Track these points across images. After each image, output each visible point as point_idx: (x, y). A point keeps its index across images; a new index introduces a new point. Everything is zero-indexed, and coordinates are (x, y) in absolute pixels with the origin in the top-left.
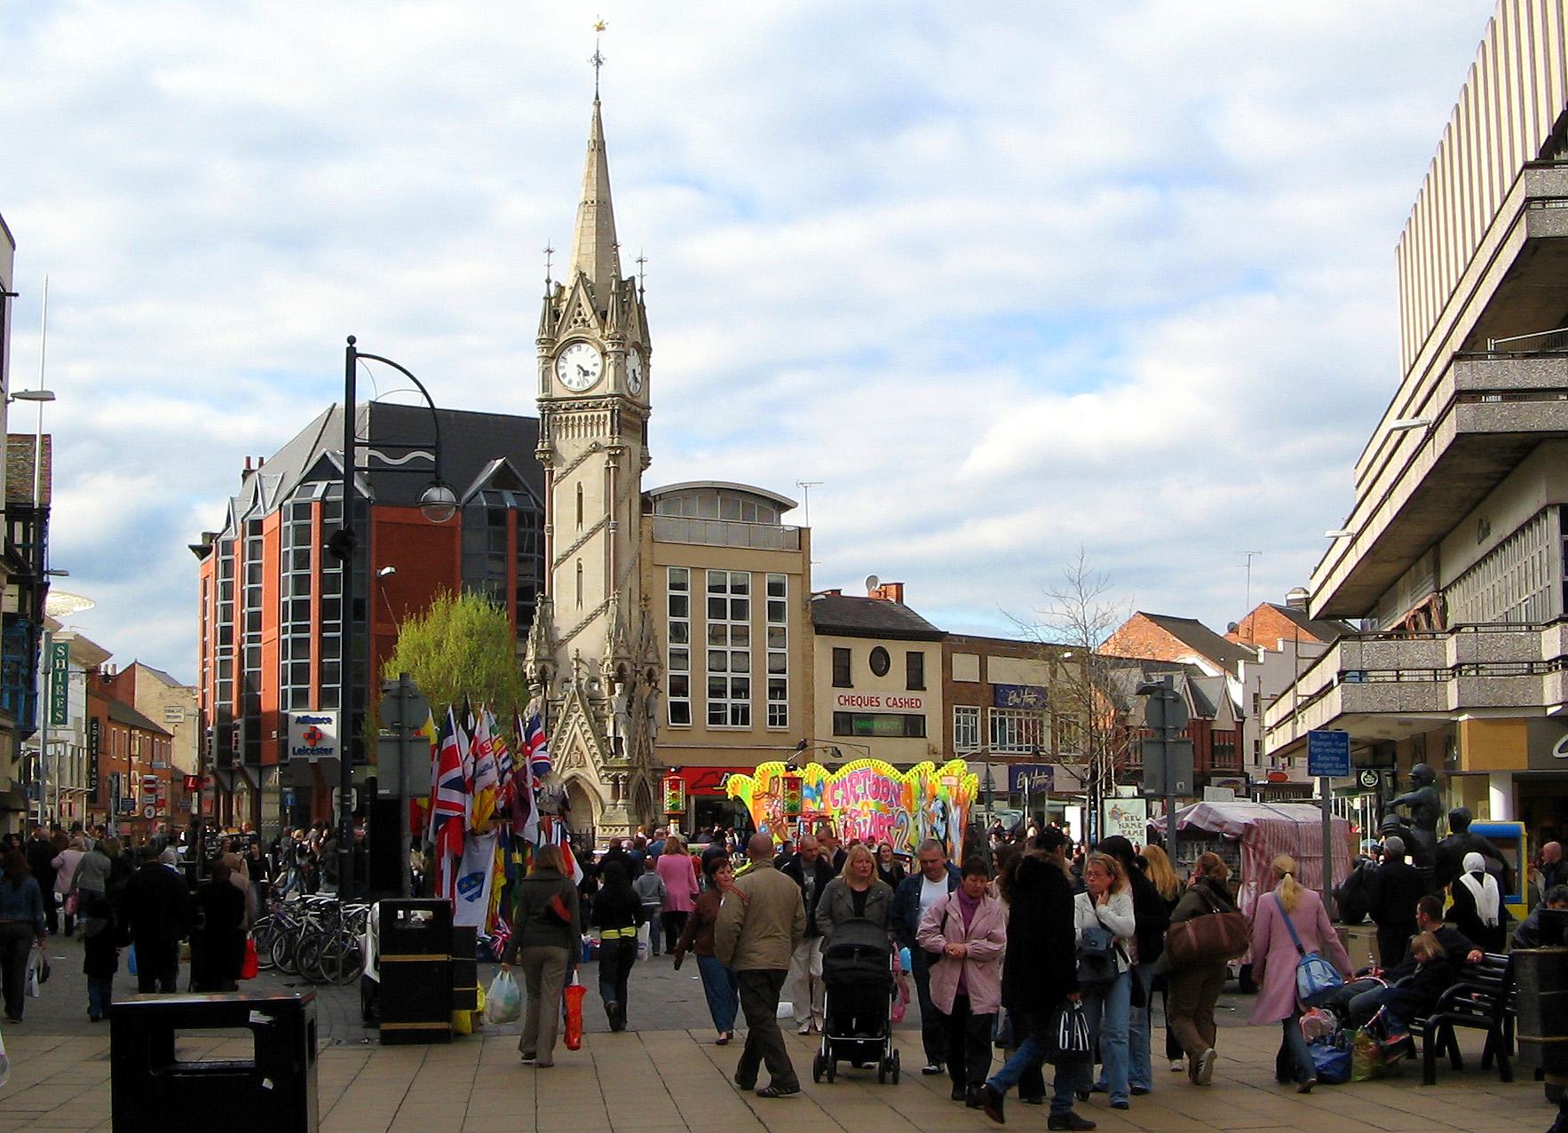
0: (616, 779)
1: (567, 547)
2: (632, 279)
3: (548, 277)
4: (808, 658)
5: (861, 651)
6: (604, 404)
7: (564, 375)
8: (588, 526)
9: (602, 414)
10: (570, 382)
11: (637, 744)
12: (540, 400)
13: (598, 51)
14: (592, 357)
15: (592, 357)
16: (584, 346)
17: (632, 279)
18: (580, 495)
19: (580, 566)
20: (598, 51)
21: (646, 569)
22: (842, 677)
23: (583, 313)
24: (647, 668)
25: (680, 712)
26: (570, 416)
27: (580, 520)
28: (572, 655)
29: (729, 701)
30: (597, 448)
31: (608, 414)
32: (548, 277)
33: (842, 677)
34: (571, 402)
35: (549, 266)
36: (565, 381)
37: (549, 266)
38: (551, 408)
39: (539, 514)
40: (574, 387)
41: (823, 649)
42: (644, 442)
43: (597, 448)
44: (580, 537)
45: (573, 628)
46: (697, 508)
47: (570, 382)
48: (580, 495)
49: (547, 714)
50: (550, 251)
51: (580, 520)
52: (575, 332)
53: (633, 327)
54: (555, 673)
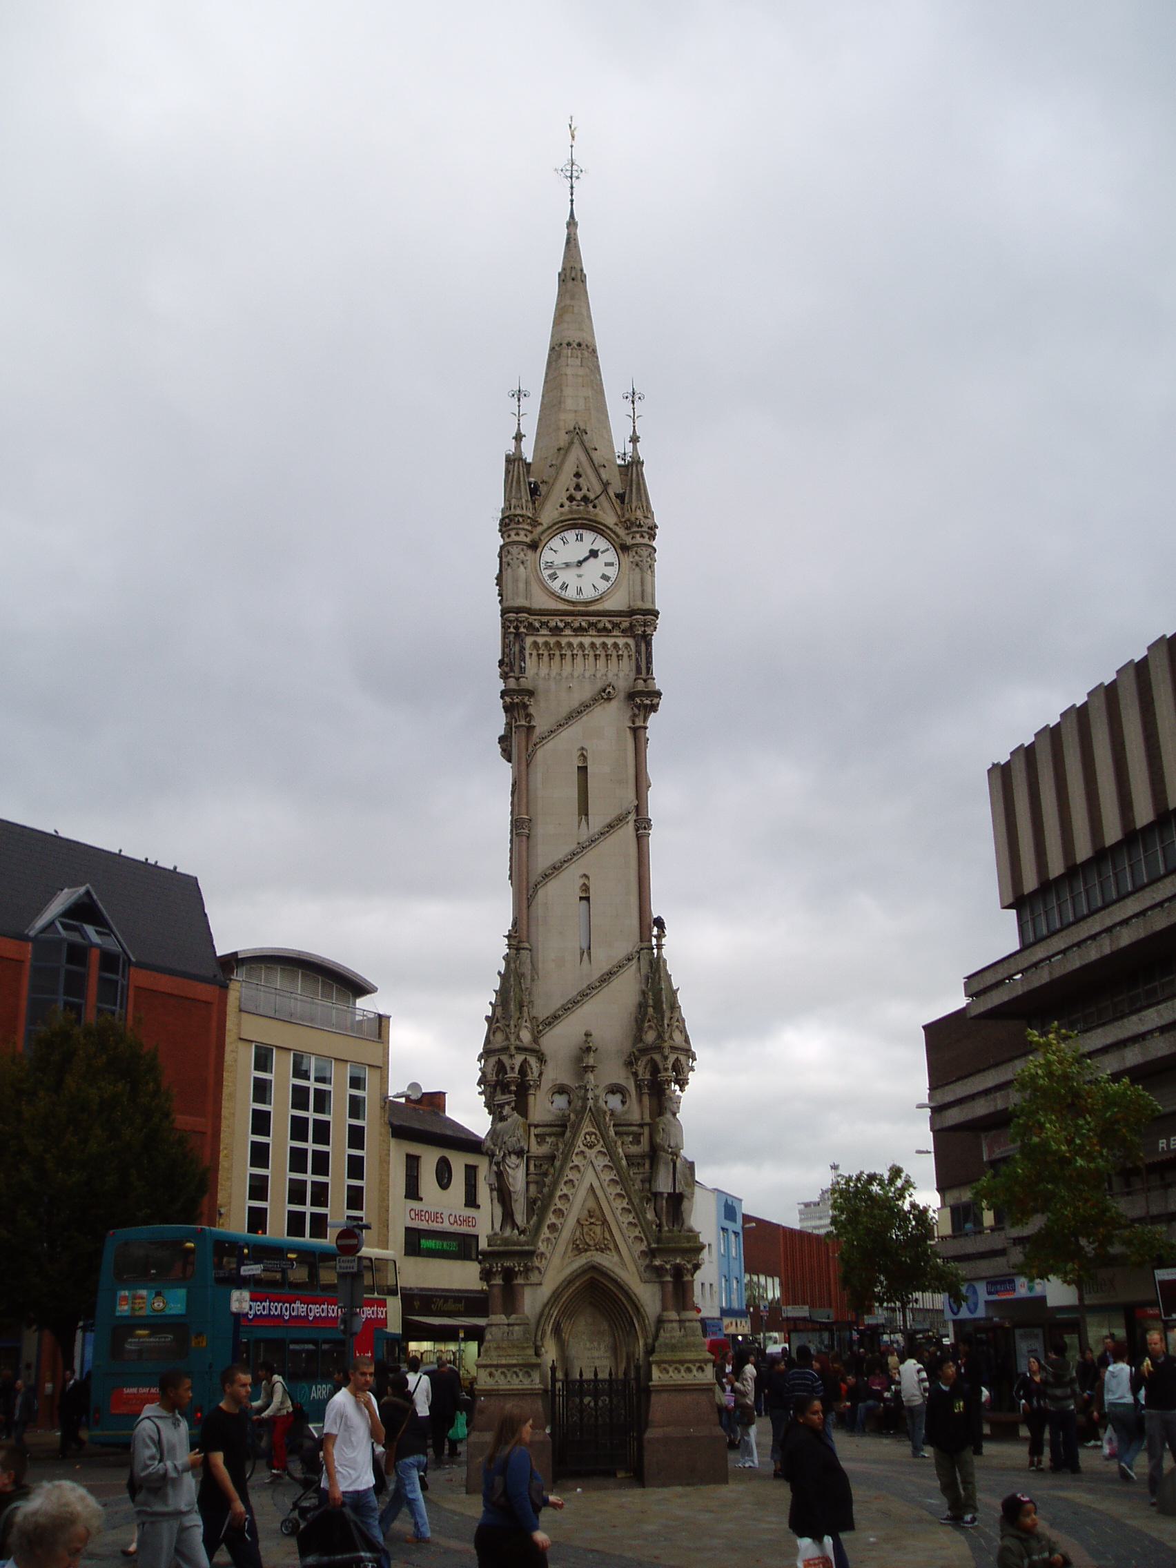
3: (519, 429)
4: (384, 1162)
5: (430, 1158)
6: (625, 625)
8: (598, 820)
18: (583, 770)
21: (231, 1043)
22: (413, 1192)
25: (257, 1219)
27: (584, 810)
29: (308, 1209)
30: (604, 695)
32: (519, 429)
33: (413, 1192)
34: (569, 619)
38: (531, 624)
41: (398, 1152)
43: (604, 695)
44: (584, 837)
46: (278, 979)
48: (583, 770)
51: (584, 810)
54: (541, 1074)
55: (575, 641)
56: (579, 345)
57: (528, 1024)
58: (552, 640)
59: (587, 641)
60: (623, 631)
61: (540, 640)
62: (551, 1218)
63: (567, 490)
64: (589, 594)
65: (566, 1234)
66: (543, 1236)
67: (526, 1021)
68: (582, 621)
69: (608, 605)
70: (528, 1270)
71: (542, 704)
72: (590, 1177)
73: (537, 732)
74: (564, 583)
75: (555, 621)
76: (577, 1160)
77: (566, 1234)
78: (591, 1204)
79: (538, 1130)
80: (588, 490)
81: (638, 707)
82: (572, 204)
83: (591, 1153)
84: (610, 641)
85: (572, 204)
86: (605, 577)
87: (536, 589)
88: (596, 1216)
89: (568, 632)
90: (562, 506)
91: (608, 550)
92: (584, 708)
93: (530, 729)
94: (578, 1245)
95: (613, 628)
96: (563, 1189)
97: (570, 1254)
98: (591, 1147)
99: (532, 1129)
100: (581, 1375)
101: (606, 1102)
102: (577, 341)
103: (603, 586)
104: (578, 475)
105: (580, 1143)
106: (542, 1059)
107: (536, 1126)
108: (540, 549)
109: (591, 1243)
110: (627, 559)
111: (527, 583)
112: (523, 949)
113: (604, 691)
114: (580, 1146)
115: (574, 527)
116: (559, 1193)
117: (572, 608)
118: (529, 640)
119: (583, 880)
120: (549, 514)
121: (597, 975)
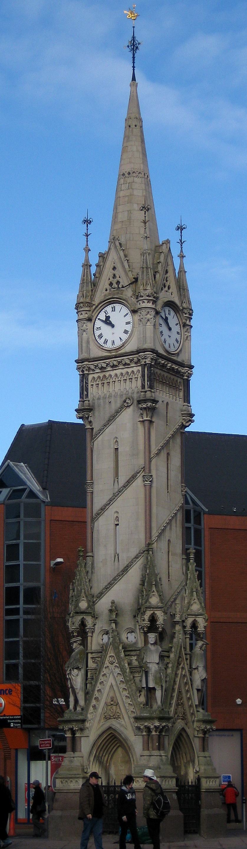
0: (148, 729)
1: (104, 502)
2: (168, 242)
7: (100, 336)
8: (122, 480)
9: (135, 369)
10: (106, 342)
11: (175, 694)
12: (77, 361)
13: (134, 37)
14: (125, 316)
15: (125, 316)
16: (118, 306)
17: (168, 242)
19: (117, 518)
20: (134, 37)
23: (117, 276)
24: (190, 621)
26: (107, 374)
28: (108, 606)
31: (140, 368)
35: (87, 235)
36: (101, 342)
37: (87, 235)
38: (89, 368)
39: (195, 511)
40: (109, 346)
42: (187, 399)
45: (110, 579)
47: (106, 342)
49: (87, 666)
50: (87, 222)
52: (110, 294)
53: (169, 288)
55: (113, 373)
56: (129, 173)
57: (85, 599)
58: (101, 375)
59: (118, 372)
60: (136, 363)
61: (96, 376)
62: (94, 702)
63: (109, 279)
64: (118, 343)
65: (100, 710)
66: (90, 712)
67: (83, 597)
68: (114, 362)
69: (128, 349)
70: (82, 730)
71: (97, 414)
72: (111, 680)
73: (94, 430)
74: (106, 339)
75: (102, 364)
76: (105, 671)
77: (100, 710)
78: (111, 694)
79: (94, 655)
80: (120, 277)
81: (141, 409)
82: (134, 70)
83: (112, 667)
84: (130, 370)
85: (134, 70)
86: (126, 332)
87: (92, 346)
88: (113, 702)
89: (109, 369)
90: (106, 290)
91: (127, 314)
92: (118, 412)
93: (92, 429)
94: (106, 716)
95: (131, 362)
96: (99, 686)
97: (102, 721)
98: (112, 664)
99: (89, 655)
100: (115, 783)
101: (127, 638)
102: (128, 172)
103: (125, 337)
104: (114, 268)
105: (107, 662)
106: (95, 617)
107: (92, 653)
108: (93, 321)
109: (112, 715)
110: (137, 317)
111: (88, 342)
112: (88, 556)
113: (125, 401)
114: (107, 663)
115: (110, 303)
116: (97, 689)
117: (109, 354)
118: (90, 377)
119: (116, 515)
120: (98, 298)
121: (121, 568)
